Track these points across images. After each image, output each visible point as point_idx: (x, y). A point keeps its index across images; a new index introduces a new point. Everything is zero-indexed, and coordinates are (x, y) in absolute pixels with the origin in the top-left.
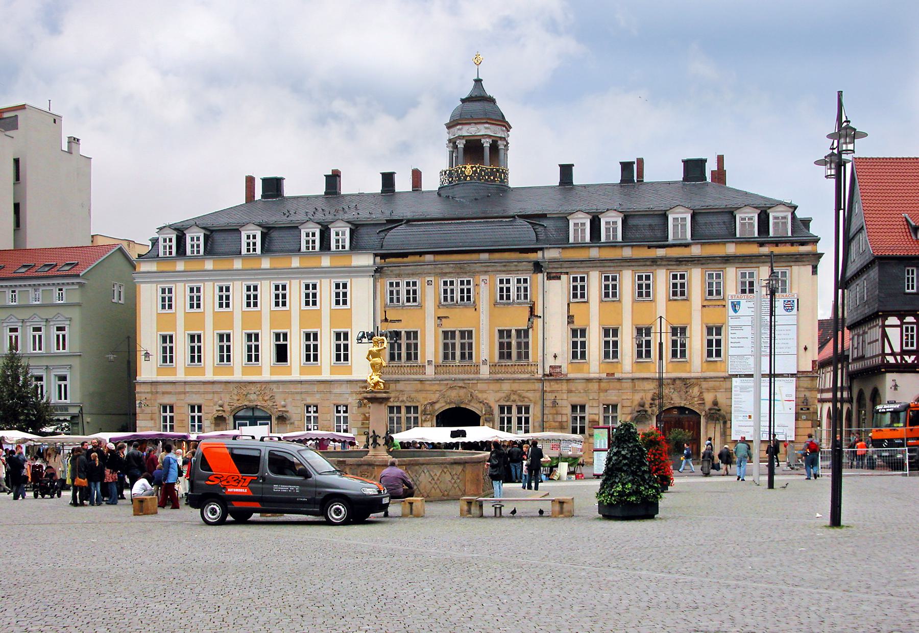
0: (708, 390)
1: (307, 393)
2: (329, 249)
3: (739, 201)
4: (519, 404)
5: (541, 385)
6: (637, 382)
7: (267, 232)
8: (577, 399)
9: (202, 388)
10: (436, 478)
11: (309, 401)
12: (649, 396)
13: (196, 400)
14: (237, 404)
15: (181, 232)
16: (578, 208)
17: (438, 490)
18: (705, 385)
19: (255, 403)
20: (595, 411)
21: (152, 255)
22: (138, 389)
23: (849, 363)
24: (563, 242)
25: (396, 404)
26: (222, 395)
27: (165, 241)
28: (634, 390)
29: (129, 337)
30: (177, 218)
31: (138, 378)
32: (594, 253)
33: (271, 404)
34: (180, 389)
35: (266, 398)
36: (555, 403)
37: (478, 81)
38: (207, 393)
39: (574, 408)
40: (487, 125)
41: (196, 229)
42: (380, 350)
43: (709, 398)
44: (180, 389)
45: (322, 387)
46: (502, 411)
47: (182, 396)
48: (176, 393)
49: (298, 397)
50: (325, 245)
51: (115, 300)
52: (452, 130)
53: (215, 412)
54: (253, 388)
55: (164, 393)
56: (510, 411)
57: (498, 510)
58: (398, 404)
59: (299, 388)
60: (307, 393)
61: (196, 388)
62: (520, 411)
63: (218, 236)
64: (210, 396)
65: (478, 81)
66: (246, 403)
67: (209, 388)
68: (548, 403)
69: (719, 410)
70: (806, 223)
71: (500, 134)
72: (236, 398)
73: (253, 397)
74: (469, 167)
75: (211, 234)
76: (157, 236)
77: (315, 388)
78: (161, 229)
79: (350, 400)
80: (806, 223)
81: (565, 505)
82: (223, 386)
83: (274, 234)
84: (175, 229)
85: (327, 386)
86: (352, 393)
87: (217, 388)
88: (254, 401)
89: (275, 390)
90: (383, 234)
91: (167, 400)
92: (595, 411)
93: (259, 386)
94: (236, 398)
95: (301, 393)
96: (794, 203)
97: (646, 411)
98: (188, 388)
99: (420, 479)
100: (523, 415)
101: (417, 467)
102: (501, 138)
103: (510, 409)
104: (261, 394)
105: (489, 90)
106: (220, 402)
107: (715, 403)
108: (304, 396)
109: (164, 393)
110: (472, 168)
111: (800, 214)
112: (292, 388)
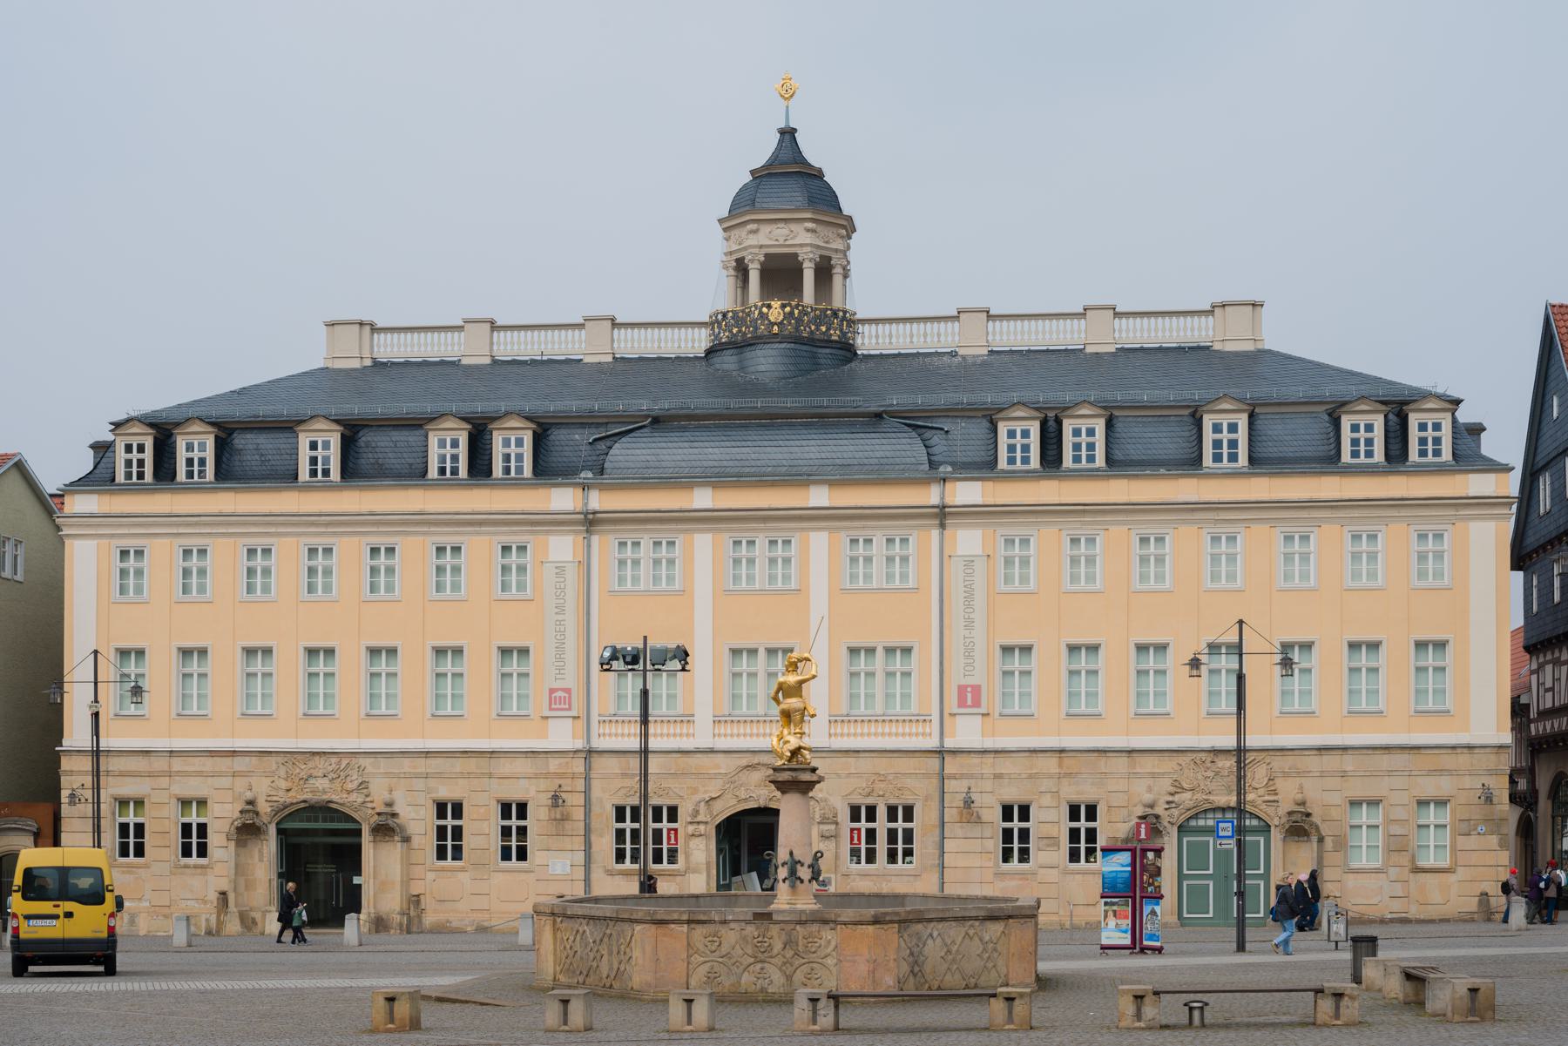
0: (1286, 775)
1: (440, 776)
2: (489, 473)
3: (1353, 390)
4: (893, 801)
5: (934, 762)
6: (1138, 758)
7: (352, 433)
8: (1014, 795)
9: (209, 764)
10: (954, 948)
11: (446, 793)
12: (1166, 785)
13: (193, 788)
15: (164, 432)
16: (1015, 396)
17: (957, 976)
18: (1278, 763)
19: (325, 797)
20: (1052, 815)
21: (99, 478)
22: (66, 764)
23: (1530, 721)
24: (986, 467)
26: (254, 780)
27: (129, 449)
28: (1132, 776)
29: (96, 652)
30: (160, 399)
31: (67, 743)
32: (1049, 491)
33: (360, 800)
34: (160, 764)
35: (350, 786)
36: (968, 803)
37: (788, 134)
38: (220, 774)
39: (1007, 813)
40: (810, 225)
41: (197, 427)
42: (801, 682)
43: (1288, 792)
44: (160, 764)
45: (472, 764)
46: (855, 817)
47: (164, 781)
48: (151, 775)
49: (420, 784)
50: (479, 465)
51: (7, 573)
52: (735, 233)
54: (321, 765)
55: (122, 774)
56: (871, 816)
57: (1196, 1014)
59: (422, 765)
60: (440, 776)
62: (892, 816)
63: (246, 441)
64: (225, 782)
65: (788, 134)
66: (305, 797)
67: (223, 764)
68: (954, 801)
69: (1308, 815)
70: (1476, 430)
71: (838, 244)
73: (322, 784)
74: (776, 304)
75: (226, 434)
76: (110, 437)
77: (459, 765)
78: (117, 425)
79: (532, 793)
80: (1476, 430)
81: (1345, 1002)
83: (365, 438)
84: (151, 425)
85: (484, 762)
87: (240, 764)
88: (325, 792)
89: (369, 769)
90: (602, 446)
91: (129, 789)
92: (1052, 815)
93: (334, 760)
94: (283, 784)
96: (1456, 394)
97: (1157, 817)
98: (177, 765)
99: (926, 951)
100: (900, 825)
101: (920, 926)
102: (836, 251)
103: (871, 814)
104: (337, 776)
105: (813, 153)
106: (249, 795)
107: (1303, 803)
108: (432, 783)
109: (122, 774)
110: (783, 306)
111: (1465, 415)
112: (406, 765)
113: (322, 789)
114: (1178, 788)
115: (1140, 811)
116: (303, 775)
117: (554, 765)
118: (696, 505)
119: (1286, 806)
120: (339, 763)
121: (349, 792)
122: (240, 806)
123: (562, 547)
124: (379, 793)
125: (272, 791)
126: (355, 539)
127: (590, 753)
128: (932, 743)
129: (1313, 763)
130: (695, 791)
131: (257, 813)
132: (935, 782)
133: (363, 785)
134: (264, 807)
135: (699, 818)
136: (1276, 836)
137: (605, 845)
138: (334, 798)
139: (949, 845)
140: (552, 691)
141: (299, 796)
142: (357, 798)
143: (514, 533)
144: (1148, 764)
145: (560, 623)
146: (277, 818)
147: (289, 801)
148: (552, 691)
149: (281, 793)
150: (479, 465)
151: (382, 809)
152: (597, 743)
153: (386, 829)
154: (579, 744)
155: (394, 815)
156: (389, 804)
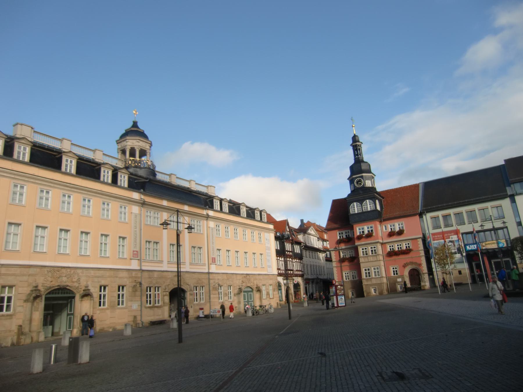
1: (102, 277)
5: (207, 275)
9: (18, 271)
14: (48, 284)
25: (157, 285)
35: (74, 280)
38: (23, 275)
45: (112, 273)
49: (96, 280)
50: (115, 181)
53: (82, 292)
58: (150, 285)
60: (102, 277)
61: (13, 271)
64: (25, 278)
72: (50, 279)
73: (64, 279)
77: (108, 273)
82: (38, 270)
86: (130, 277)
87: (31, 271)
88: (65, 282)
89: (81, 274)
93: (69, 270)
94: (50, 279)
95: (98, 277)
107: (257, 285)
112: (92, 272)
113: (64, 281)
114: (243, 281)
115: (238, 287)
116: (58, 276)
117: (134, 274)
118: (164, 204)
119: (255, 286)
120: (70, 272)
121: (73, 282)
122: (30, 289)
123: (136, 209)
124: (83, 283)
125: (45, 283)
126: (79, 195)
127: (143, 271)
128: (207, 271)
129: (258, 277)
130: (164, 282)
131: (39, 290)
132: (208, 280)
133: (79, 280)
134: (40, 288)
135: (167, 290)
136: (254, 292)
137: (144, 298)
138: (69, 284)
139: (212, 296)
140: (134, 251)
141: (56, 284)
142: (76, 285)
143: (124, 203)
144: (238, 276)
145: (136, 231)
146: (46, 293)
147: (52, 286)
148: (134, 251)
149: (48, 283)
150: (115, 181)
151: (84, 288)
152: (144, 268)
153: (87, 294)
154: (139, 268)
155: (89, 290)
156: (87, 287)
